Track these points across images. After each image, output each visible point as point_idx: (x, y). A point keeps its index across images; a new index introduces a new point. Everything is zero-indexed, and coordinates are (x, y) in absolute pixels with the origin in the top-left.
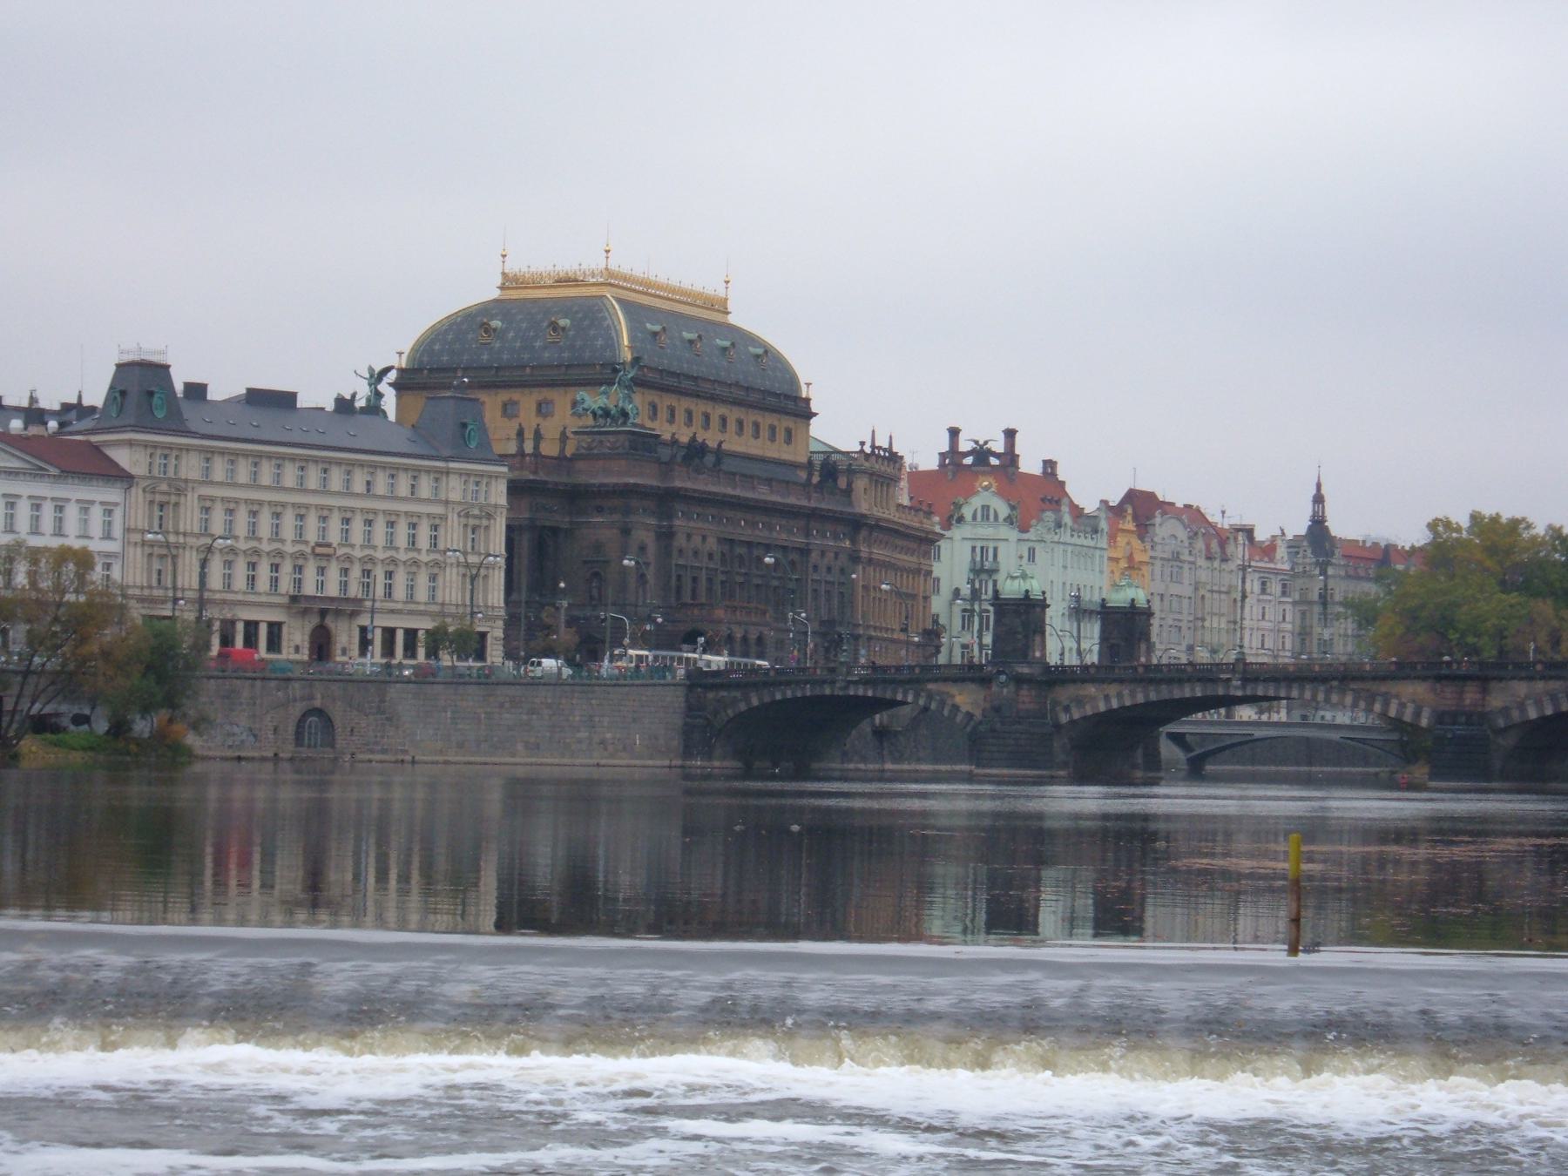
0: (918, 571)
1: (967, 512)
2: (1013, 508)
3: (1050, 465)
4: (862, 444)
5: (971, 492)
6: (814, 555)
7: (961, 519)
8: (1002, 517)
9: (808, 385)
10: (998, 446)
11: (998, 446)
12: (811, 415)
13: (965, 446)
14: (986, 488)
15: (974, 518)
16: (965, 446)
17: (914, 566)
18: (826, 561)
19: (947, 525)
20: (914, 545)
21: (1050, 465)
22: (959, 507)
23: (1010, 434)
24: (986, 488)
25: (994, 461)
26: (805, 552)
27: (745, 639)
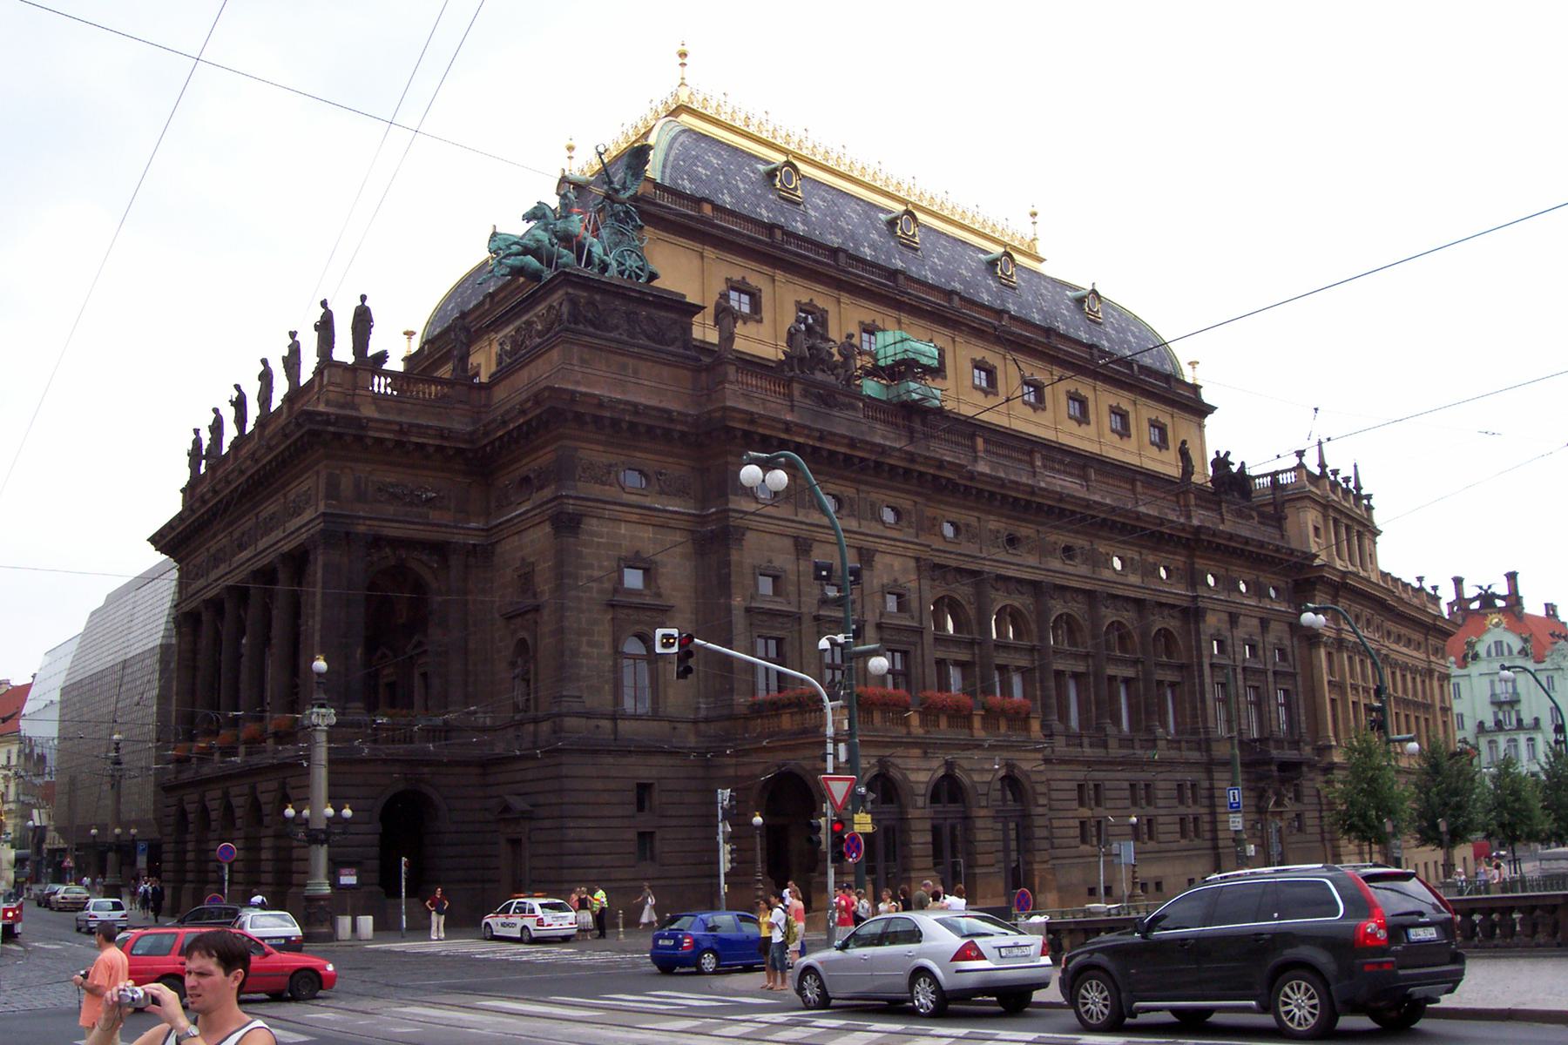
0: (1430, 672)
1: (1481, 649)
2: (1525, 641)
3: (1550, 607)
4: (1300, 454)
5: (1483, 630)
6: (1213, 621)
7: (1476, 657)
8: (1515, 651)
9: (1193, 364)
10: (1502, 588)
11: (1502, 588)
12: (1206, 410)
13: (1470, 592)
14: (1497, 625)
15: (1489, 654)
16: (1470, 592)
17: (1421, 665)
18: (1241, 633)
19: (1463, 663)
20: (1417, 636)
21: (1550, 607)
22: (1471, 645)
23: (1512, 577)
24: (1497, 625)
25: (1500, 603)
26: (1192, 614)
27: (949, 789)
